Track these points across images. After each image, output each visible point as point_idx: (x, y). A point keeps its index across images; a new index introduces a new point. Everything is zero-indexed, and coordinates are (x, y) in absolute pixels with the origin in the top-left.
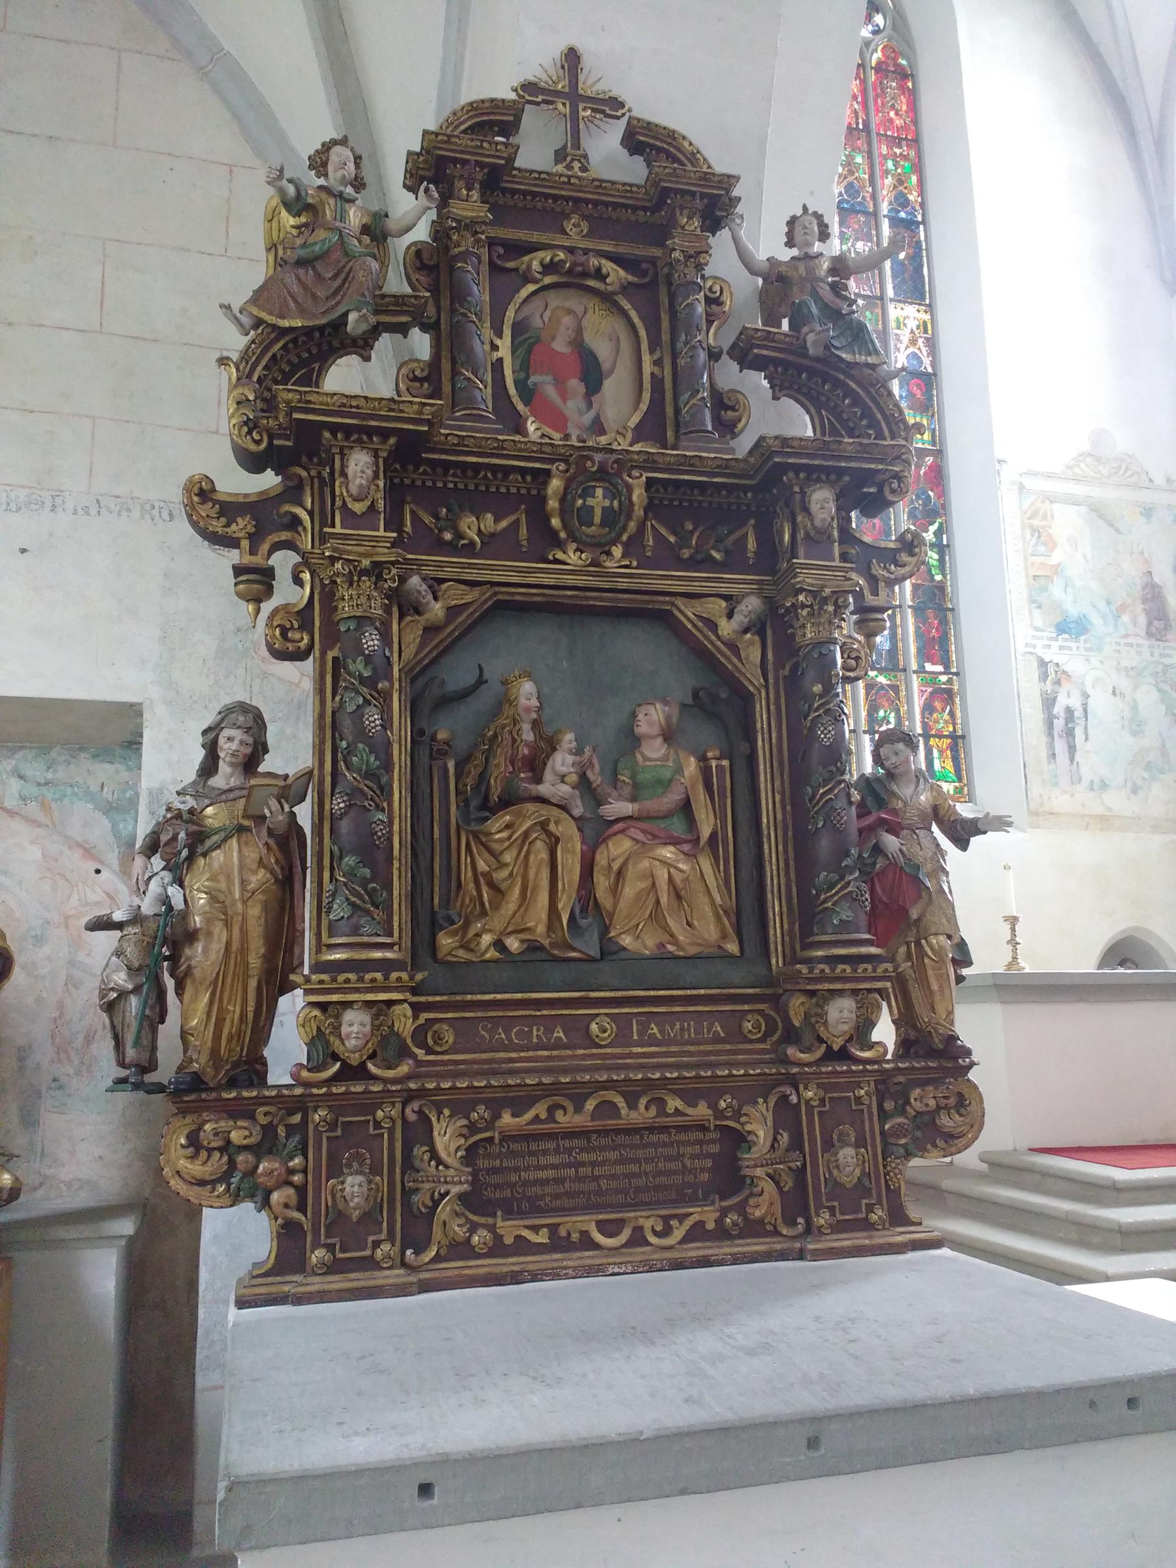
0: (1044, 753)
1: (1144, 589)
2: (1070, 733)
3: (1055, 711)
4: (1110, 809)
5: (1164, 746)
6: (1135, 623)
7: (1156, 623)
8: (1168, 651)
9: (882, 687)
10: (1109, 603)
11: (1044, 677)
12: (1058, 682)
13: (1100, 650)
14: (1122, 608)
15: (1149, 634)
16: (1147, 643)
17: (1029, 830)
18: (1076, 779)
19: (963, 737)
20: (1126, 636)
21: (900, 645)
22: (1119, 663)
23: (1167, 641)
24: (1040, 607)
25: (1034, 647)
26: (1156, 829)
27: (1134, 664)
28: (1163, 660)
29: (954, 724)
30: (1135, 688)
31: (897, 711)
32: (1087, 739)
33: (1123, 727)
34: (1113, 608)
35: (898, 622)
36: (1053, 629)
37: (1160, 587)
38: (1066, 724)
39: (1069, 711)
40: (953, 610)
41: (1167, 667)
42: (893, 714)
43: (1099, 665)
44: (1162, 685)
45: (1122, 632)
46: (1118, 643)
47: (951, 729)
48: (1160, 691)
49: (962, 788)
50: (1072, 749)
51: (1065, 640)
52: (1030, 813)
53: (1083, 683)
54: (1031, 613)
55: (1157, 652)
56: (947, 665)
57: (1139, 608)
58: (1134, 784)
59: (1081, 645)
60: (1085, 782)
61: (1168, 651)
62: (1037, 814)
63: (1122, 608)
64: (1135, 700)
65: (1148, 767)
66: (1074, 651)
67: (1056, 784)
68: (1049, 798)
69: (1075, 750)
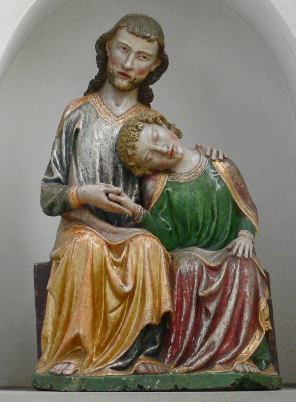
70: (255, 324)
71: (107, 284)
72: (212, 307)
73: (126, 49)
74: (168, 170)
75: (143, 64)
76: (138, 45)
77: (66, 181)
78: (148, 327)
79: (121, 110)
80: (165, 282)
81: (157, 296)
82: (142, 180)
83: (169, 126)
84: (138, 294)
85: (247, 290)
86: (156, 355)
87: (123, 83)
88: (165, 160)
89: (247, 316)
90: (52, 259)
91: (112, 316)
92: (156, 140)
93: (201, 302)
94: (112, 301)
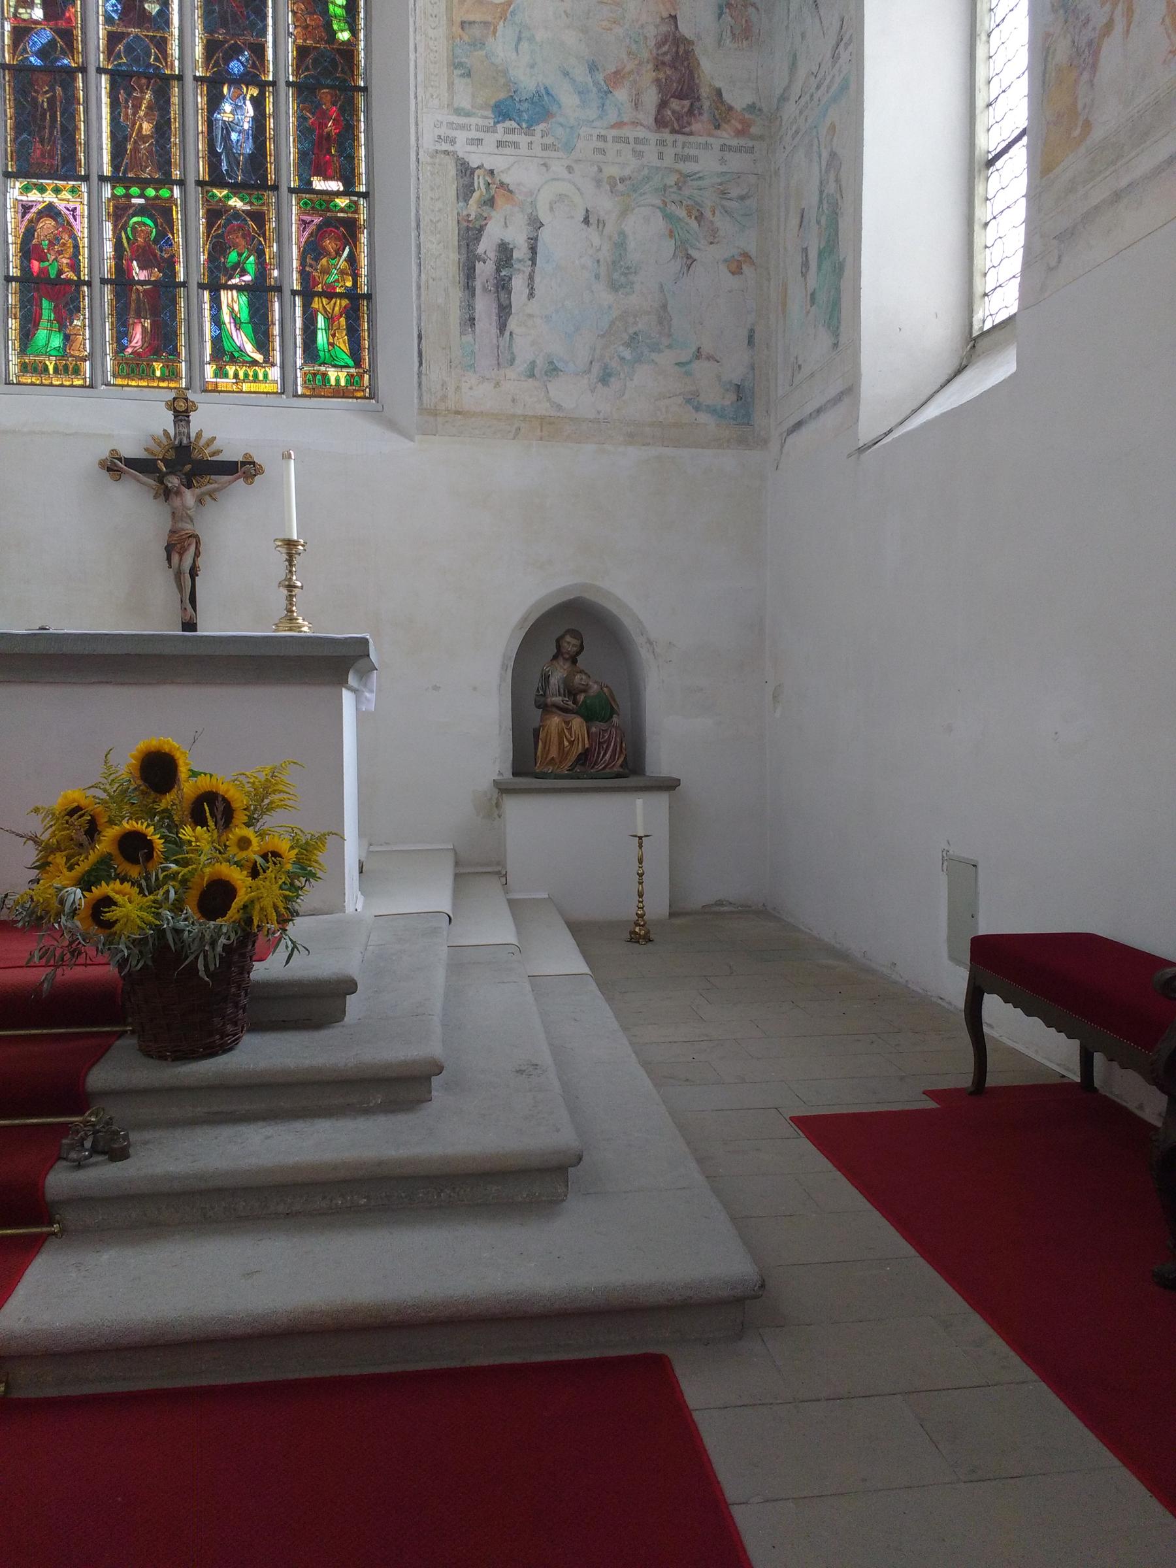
0: (455, 315)
1: (660, 45)
2: (503, 286)
3: (480, 250)
4: (559, 407)
5: (664, 307)
6: (637, 104)
7: (675, 104)
8: (692, 152)
9: (236, 214)
10: (593, 68)
11: (466, 192)
12: (490, 202)
13: (569, 148)
14: (617, 77)
15: (660, 122)
16: (653, 137)
17: (417, 437)
18: (504, 358)
19: (368, 297)
20: (619, 125)
21: (270, 146)
22: (600, 170)
23: (691, 134)
24: (469, 75)
25: (453, 142)
26: (632, 438)
27: (626, 172)
28: (681, 166)
29: (355, 276)
30: (624, 212)
31: (260, 254)
32: (531, 295)
33: (597, 277)
34: (600, 77)
35: (269, 109)
36: (489, 113)
37: (691, 43)
38: (498, 270)
39: (505, 252)
40: (365, 89)
41: (685, 177)
42: (252, 258)
43: (565, 174)
44: (672, 208)
45: (612, 117)
46: (603, 138)
47: (349, 284)
48: (668, 217)
49: (361, 377)
50: (504, 311)
51: (507, 131)
52: (423, 410)
53: (533, 204)
54: (451, 85)
55: (669, 152)
56: (349, 179)
57: (648, 75)
58: (605, 367)
59: (537, 139)
60: (521, 365)
61: (692, 152)
62: (434, 413)
63: (617, 77)
64: (622, 234)
65: (633, 341)
66: (524, 150)
67: (472, 366)
68: (458, 388)
69: (510, 313)
71: (565, 739)
72: (605, 747)
73: (569, 643)
74: (584, 691)
76: (574, 641)
77: (544, 695)
79: (565, 667)
80: (586, 736)
82: (575, 695)
83: (586, 674)
84: (576, 742)
85: (618, 739)
86: (583, 764)
87: (567, 656)
89: (618, 749)
90: (540, 726)
91: (566, 749)
94: (566, 743)
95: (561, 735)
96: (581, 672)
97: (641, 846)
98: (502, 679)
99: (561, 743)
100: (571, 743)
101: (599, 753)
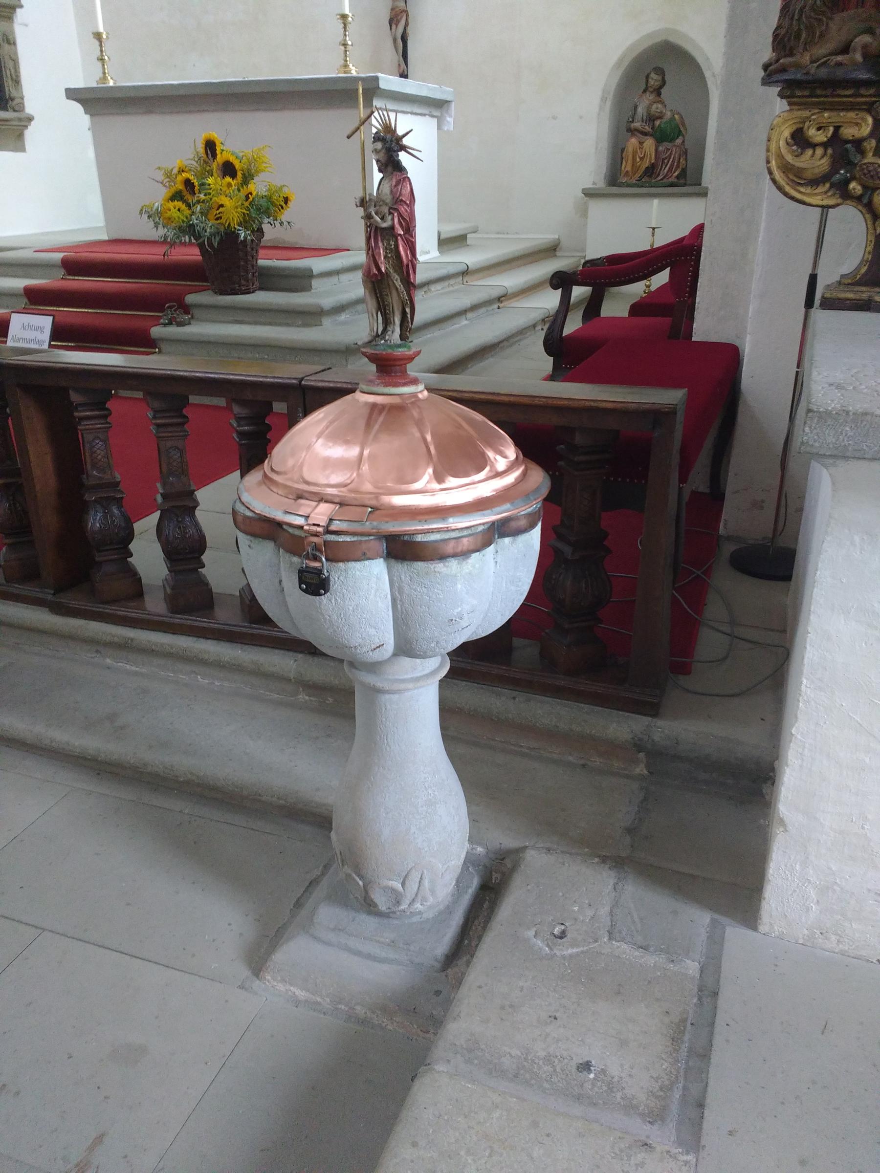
70: (678, 166)
74: (660, 118)
75: (656, 83)
78: (648, 167)
81: (651, 157)
82: (654, 121)
85: (677, 156)
86: (650, 176)
88: (660, 114)
92: (657, 108)
93: (663, 160)
95: (635, 153)
96: (662, 102)
97: (653, 235)
98: (601, 108)
99: (634, 160)
100: (642, 159)
101: (662, 167)
